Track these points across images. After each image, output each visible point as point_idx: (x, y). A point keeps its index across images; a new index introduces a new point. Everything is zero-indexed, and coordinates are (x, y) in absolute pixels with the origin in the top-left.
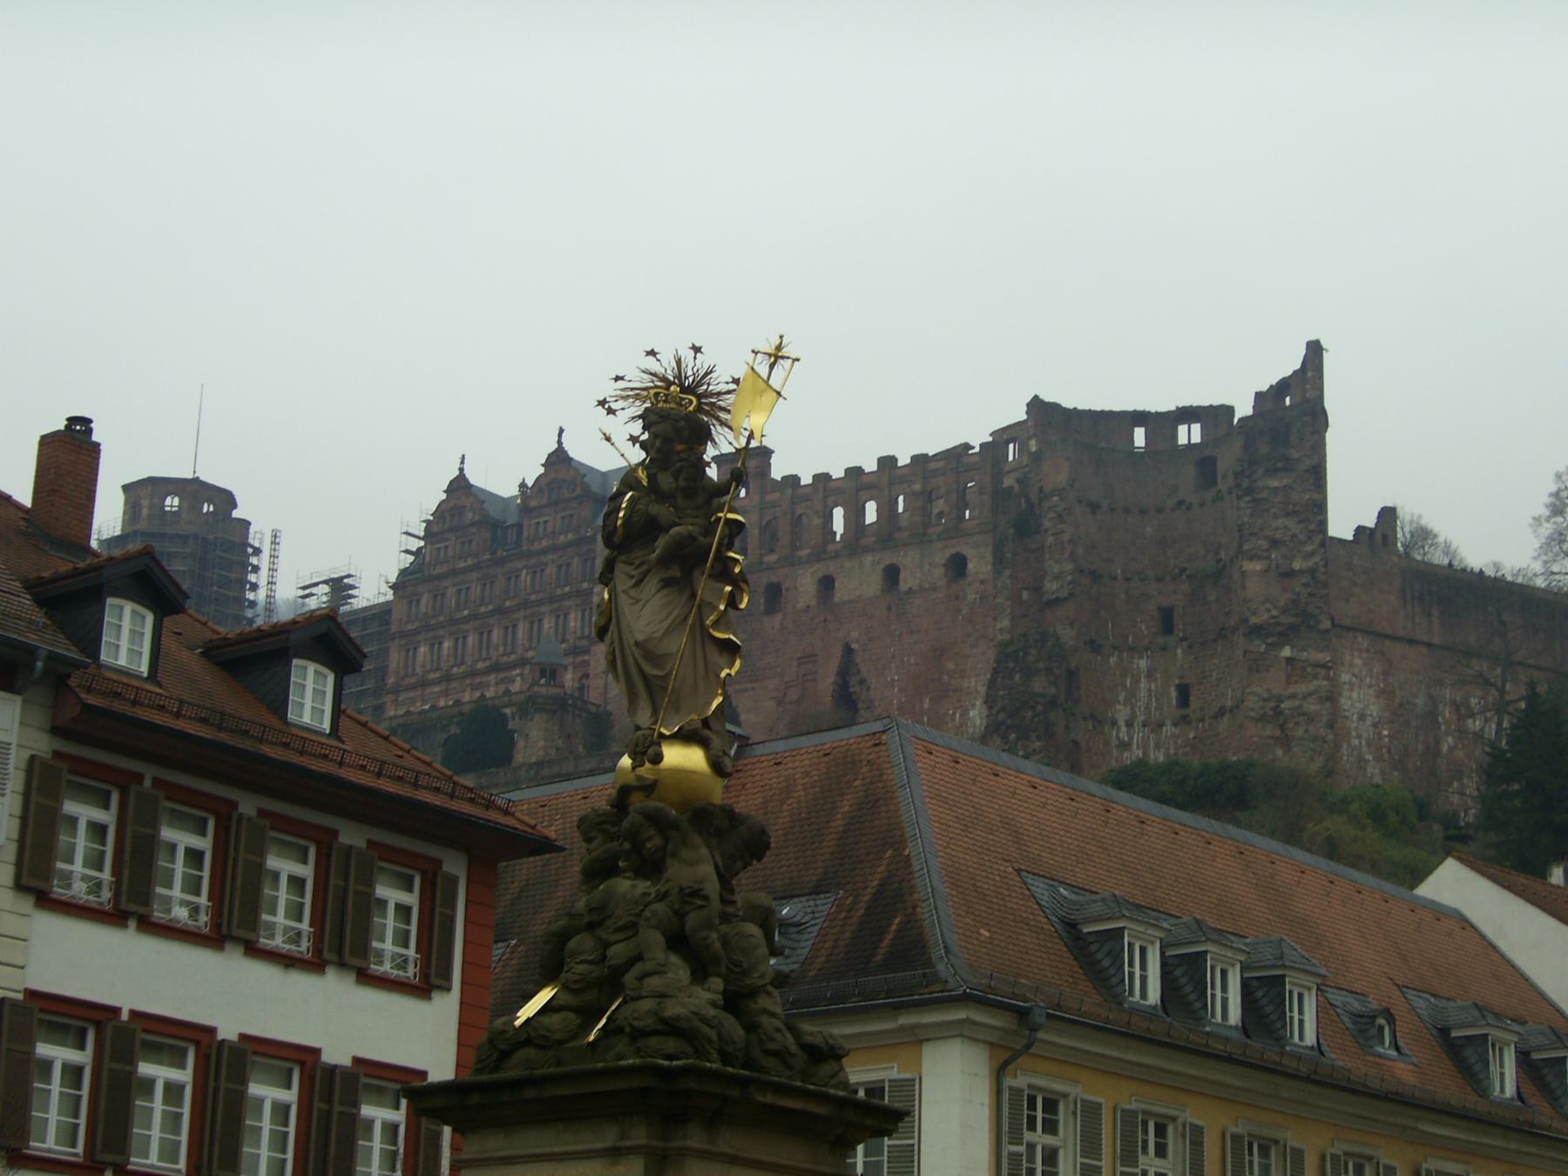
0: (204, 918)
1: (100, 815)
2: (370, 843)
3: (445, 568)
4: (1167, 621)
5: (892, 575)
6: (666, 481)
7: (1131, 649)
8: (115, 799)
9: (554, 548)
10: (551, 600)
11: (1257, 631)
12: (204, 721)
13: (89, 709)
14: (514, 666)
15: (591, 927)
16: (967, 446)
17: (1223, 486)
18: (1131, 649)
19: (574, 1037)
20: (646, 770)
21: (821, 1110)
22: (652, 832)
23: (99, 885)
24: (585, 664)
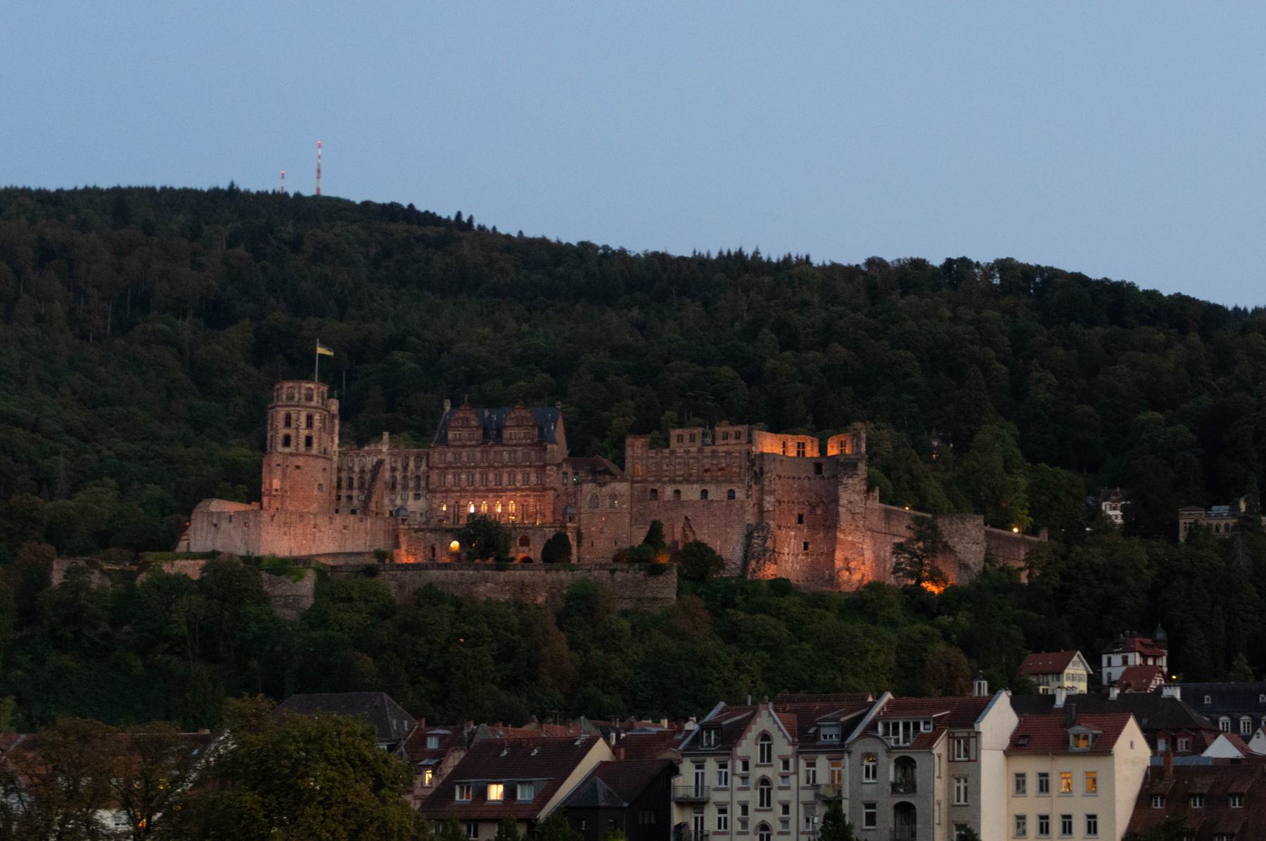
3: (459, 443)
4: (800, 519)
5: (704, 493)
17: (826, 474)
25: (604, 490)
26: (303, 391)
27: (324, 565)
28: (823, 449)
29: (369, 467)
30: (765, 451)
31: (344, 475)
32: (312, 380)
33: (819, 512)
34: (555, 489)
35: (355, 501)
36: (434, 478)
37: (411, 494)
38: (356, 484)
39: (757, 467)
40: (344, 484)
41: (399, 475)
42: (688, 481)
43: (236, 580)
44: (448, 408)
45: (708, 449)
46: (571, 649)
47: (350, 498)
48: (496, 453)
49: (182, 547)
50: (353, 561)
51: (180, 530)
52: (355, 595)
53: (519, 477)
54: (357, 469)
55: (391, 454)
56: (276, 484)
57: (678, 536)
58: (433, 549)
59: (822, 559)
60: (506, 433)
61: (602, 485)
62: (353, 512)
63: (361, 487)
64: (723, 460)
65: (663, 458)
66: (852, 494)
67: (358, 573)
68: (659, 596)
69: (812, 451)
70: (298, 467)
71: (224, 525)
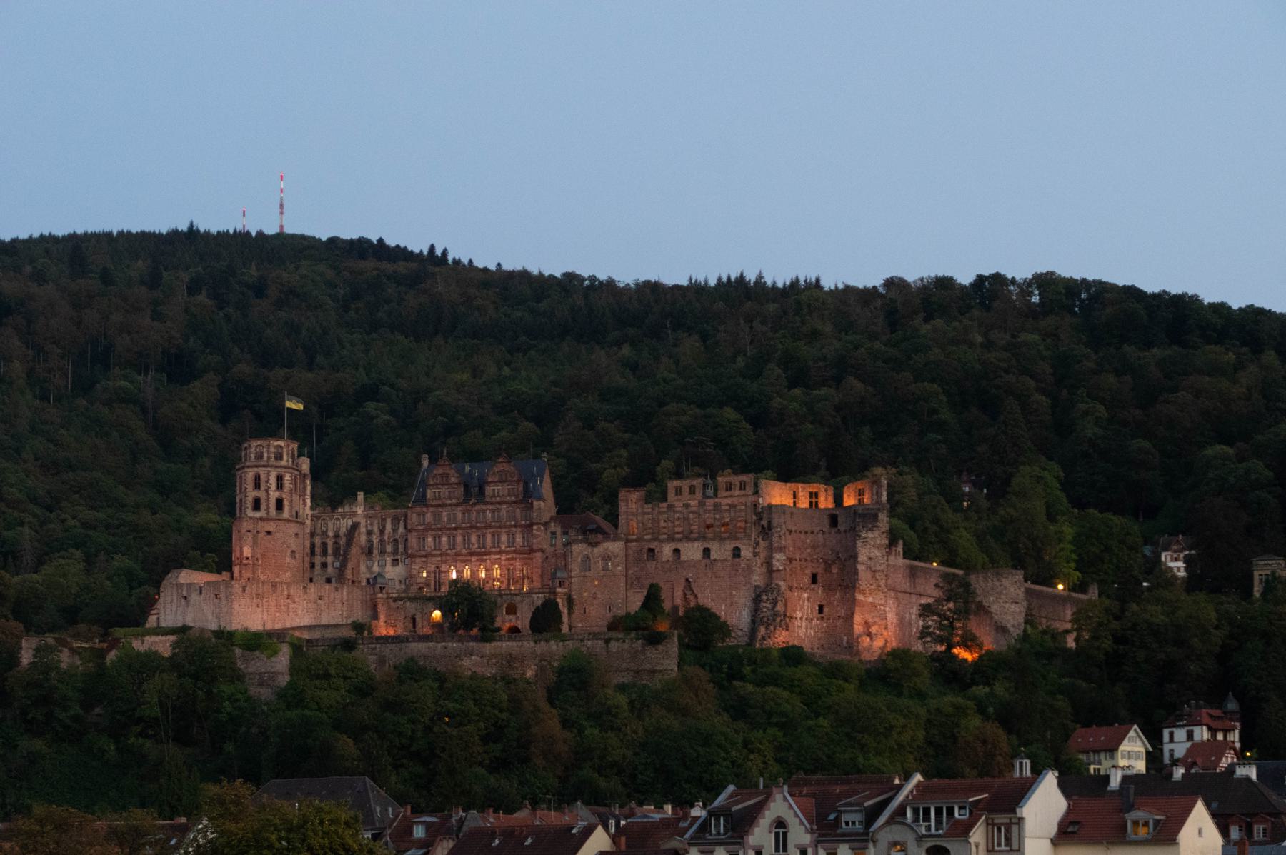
4: (814, 579)
5: (707, 552)
9: (505, 503)
14: (486, 554)
17: (842, 527)
25: (596, 550)
26: (272, 450)
27: (300, 639)
28: (838, 499)
29: (343, 530)
30: (774, 502)
31: (318, 541)
32: (282, 438)
33: (835, 570)
34: (543, 551)
35: (330, 569)
36: (413, 541)
37: (389, 560)
38: (330, 551)
39: (764, 522)
40: (318, 550)
41: (375, 539)
42: (688, 538)
43: (207, 656)
44: (425, 464)
45: (710, 502)
46: (564, 727)
47: (324, 565)
48: (478, 512)
49: (152, 621)
50: (329, 634)
51: (148, 604)
52: (333, 672)
53: (504, 538)
54: (331, 534)
55: (367, 517)
56: (247, 551)
57: (678, 601)
58: (414, 619)
59: (839, 623)
60: (489, 490)
61: (594, 545)
62: (329, 581)
63: (336, 553)
64: (726, 515)
65: (660, 513)
66: (872, 549)
67: (334, 647)
68: (660, 668)
69: (826, 502)
70: (269, 533)
71: (194, 597)
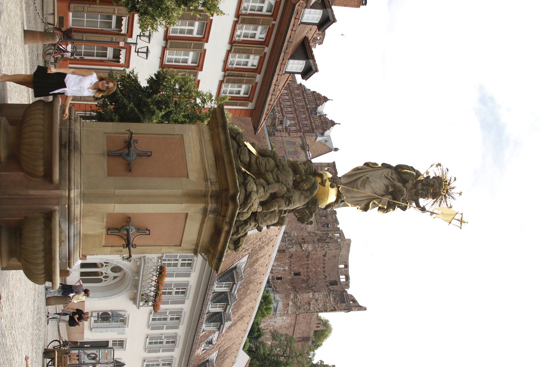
0: (237, 39)
1: (265, 10)
2: (257, 83)
4: (297, 274)
6: (420, 186)
7: (290, 265)
8: (270, 14)
9: (311, 123)
10: (299, 122)
11: (296, 297)
12: (290, 37)
13: (295, 5)
15: (277, 166)
16: (338, 224)
17: (330, 287)
18: (290, 265)
19: (241, 162)
20: (328, 183)
21: (220, 247)
22: (309, 186)
23: (246, 10)
24: (283, 131)
25: (299, 148)
